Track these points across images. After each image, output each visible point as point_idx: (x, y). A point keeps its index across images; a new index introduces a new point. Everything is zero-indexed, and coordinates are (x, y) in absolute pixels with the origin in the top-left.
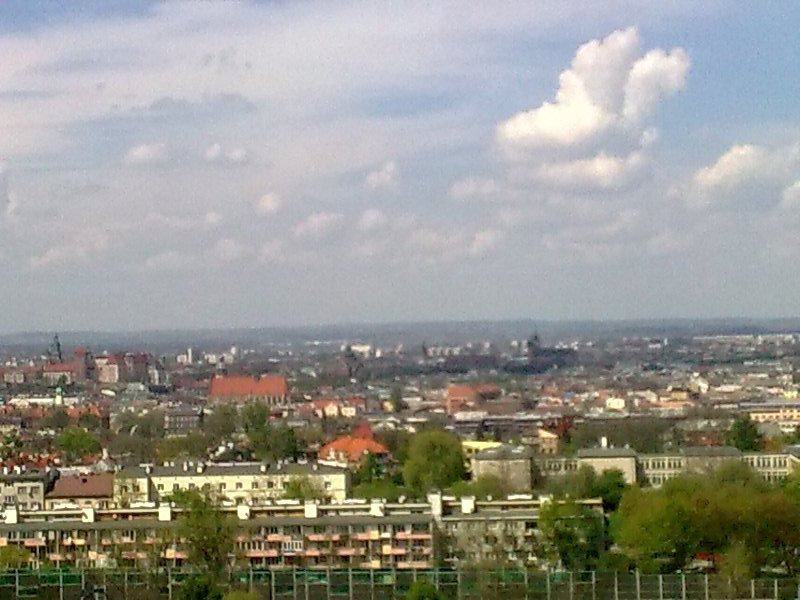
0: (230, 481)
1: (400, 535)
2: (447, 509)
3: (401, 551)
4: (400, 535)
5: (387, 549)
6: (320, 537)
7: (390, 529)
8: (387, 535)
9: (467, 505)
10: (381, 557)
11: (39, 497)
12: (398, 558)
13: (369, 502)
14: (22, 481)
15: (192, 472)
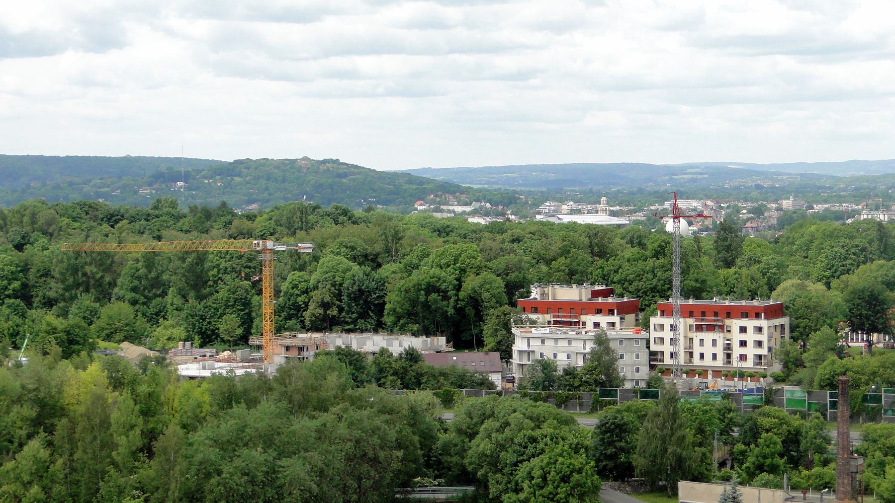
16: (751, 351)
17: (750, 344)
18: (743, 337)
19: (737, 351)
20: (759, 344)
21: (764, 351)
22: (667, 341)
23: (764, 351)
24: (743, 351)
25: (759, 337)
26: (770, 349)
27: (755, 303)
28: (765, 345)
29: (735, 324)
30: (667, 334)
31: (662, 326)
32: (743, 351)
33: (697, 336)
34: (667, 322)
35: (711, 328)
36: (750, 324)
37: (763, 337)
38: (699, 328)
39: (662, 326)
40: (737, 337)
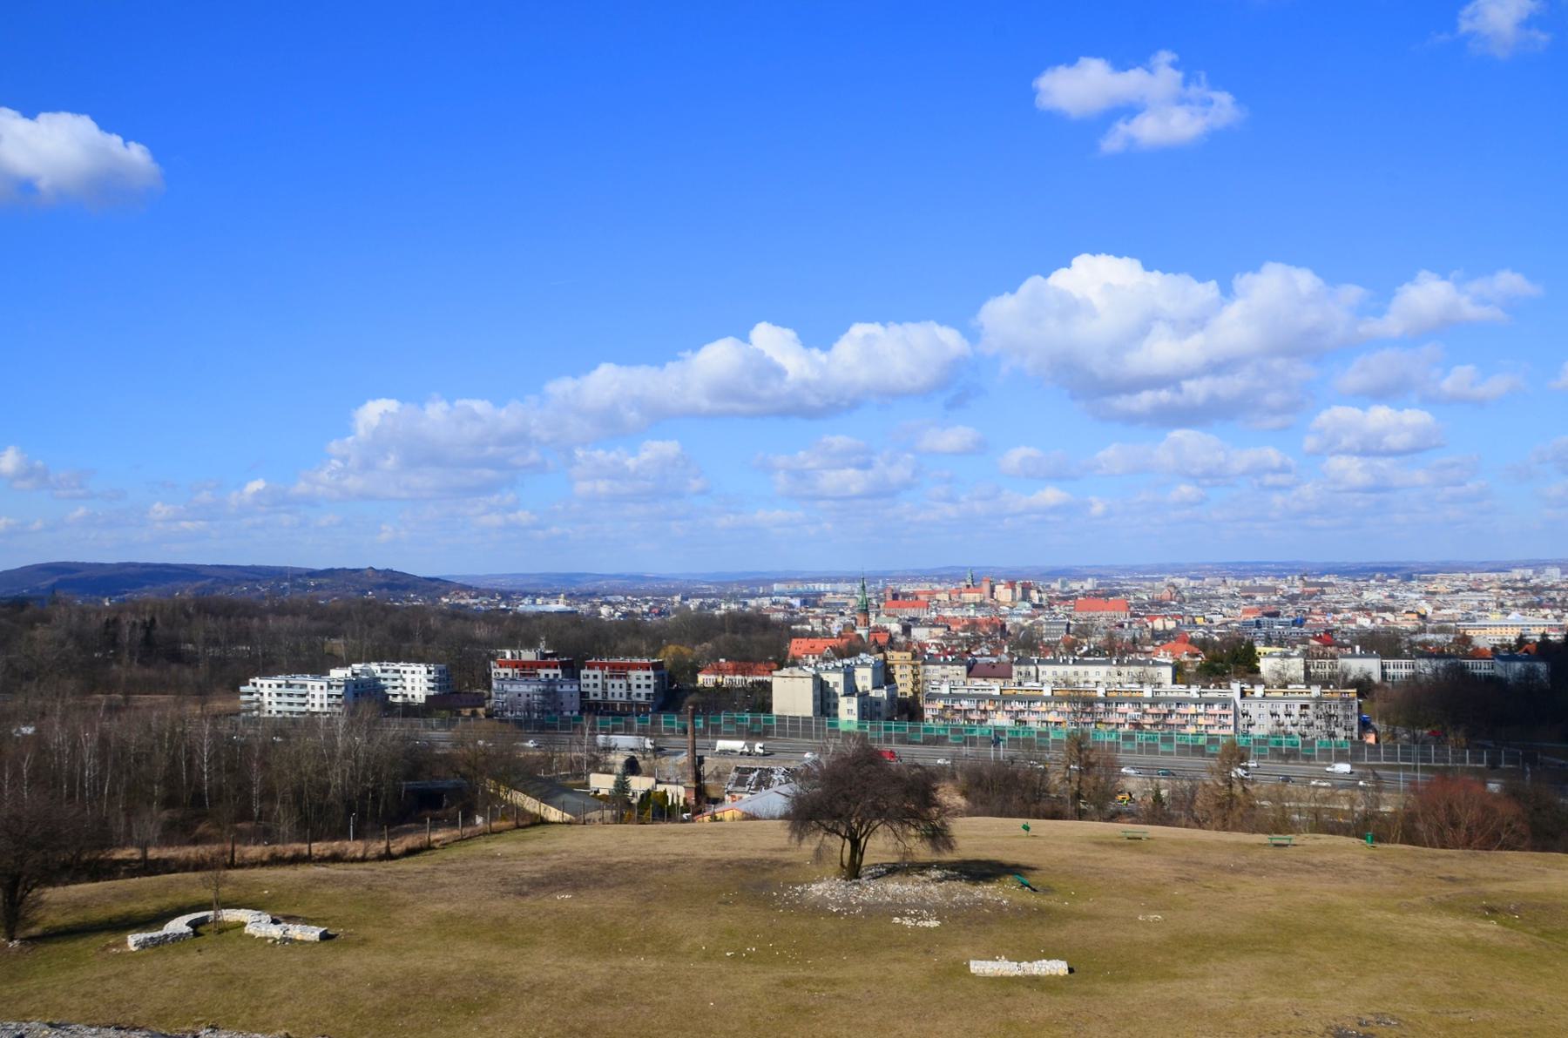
0: (1092, 669)
1: (1210, 711)
4: (1210, 711)
5: (1201, 720)
6: (1154, 710)
7: (1203, 706)
11: (964, 677)
13: (1189, 687)
15: (1065, 662)
16: (643, 691)
17: (643, 686)
19: (635, 691)
20: (648, 686)
21: (651, 691)
24: (639, 691)
25: (648, 682)
26: (655, 690)
27: (646, 661)
28: (652, 687)
29: (633, 674)
31: (588, 676)
32: (639, 691)
33: (610, 682)
34: (591, 673)
35: (619, 677)
36: (643, 674)
39: (588, 676)
40: (634, 682)
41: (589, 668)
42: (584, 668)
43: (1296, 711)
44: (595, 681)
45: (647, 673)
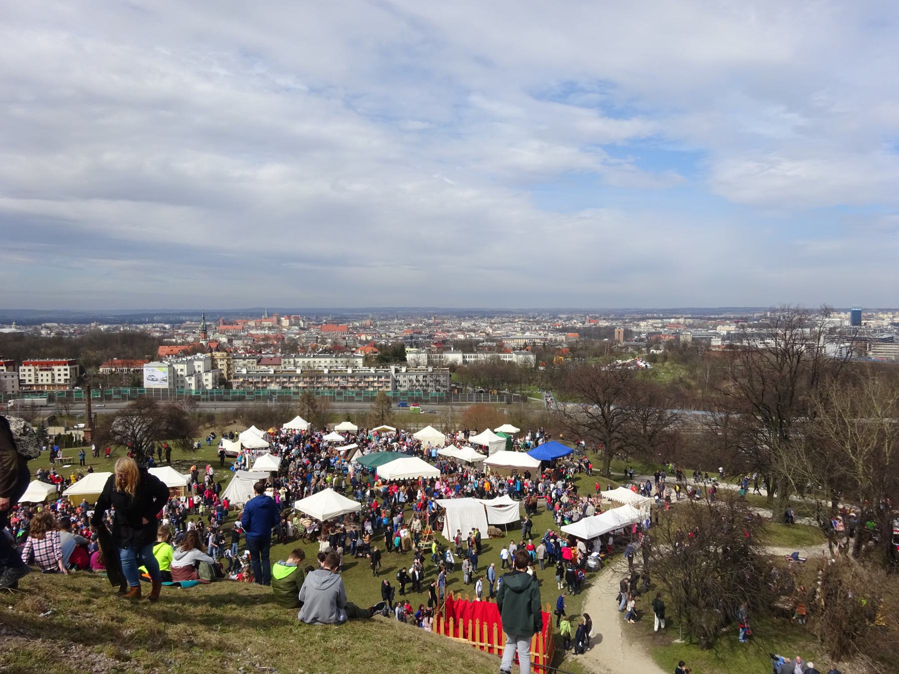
0: (323, 360)
1: (380, 380)
2: (397, 371)
3: (381, 385)
4: (380, 380)
5: (376, 384)
6: (353, 380)
7: (377, 378)
8: (376, 379)
9: (404, 369)
10: (373, 387)
11: (255, 365)
12: (379, 387)
13: (370, 368)
14: (249, 359)
15: (309, 357)
16: (63, 378)
17: (62, 375)
18: (59, 373)
19: (57, 378)
20: (66, 375)
21: (68, 377)
22: (27, 375)
23: (68, 377)
24: (60, 378)
25: (66, 372)
26: (71, 376)
27: (64, 360)
28: (69, 375)
29: (56, 368)
30: (27, 373)
31: (24, 370)
32: (60, 378)
33: (40, 373)
34: (27, 368)
36: (62, 368)
37: (68, 372)
38: (41, 370)
40: (56, 372)
41: (25, 365)
42: (21, 365)
43: (421, 378)
44: (30, 373)
45: (65, 367)
